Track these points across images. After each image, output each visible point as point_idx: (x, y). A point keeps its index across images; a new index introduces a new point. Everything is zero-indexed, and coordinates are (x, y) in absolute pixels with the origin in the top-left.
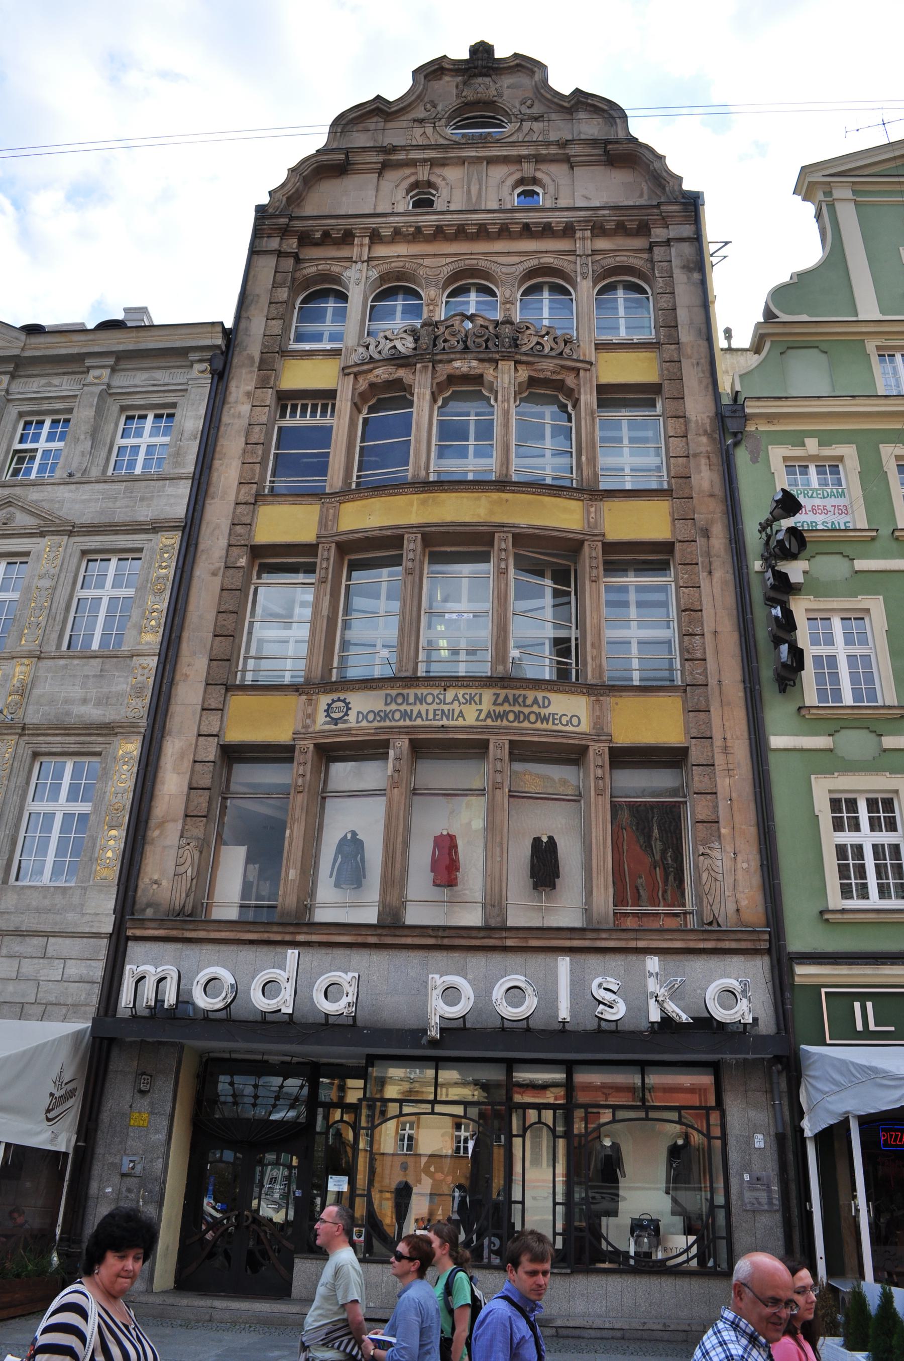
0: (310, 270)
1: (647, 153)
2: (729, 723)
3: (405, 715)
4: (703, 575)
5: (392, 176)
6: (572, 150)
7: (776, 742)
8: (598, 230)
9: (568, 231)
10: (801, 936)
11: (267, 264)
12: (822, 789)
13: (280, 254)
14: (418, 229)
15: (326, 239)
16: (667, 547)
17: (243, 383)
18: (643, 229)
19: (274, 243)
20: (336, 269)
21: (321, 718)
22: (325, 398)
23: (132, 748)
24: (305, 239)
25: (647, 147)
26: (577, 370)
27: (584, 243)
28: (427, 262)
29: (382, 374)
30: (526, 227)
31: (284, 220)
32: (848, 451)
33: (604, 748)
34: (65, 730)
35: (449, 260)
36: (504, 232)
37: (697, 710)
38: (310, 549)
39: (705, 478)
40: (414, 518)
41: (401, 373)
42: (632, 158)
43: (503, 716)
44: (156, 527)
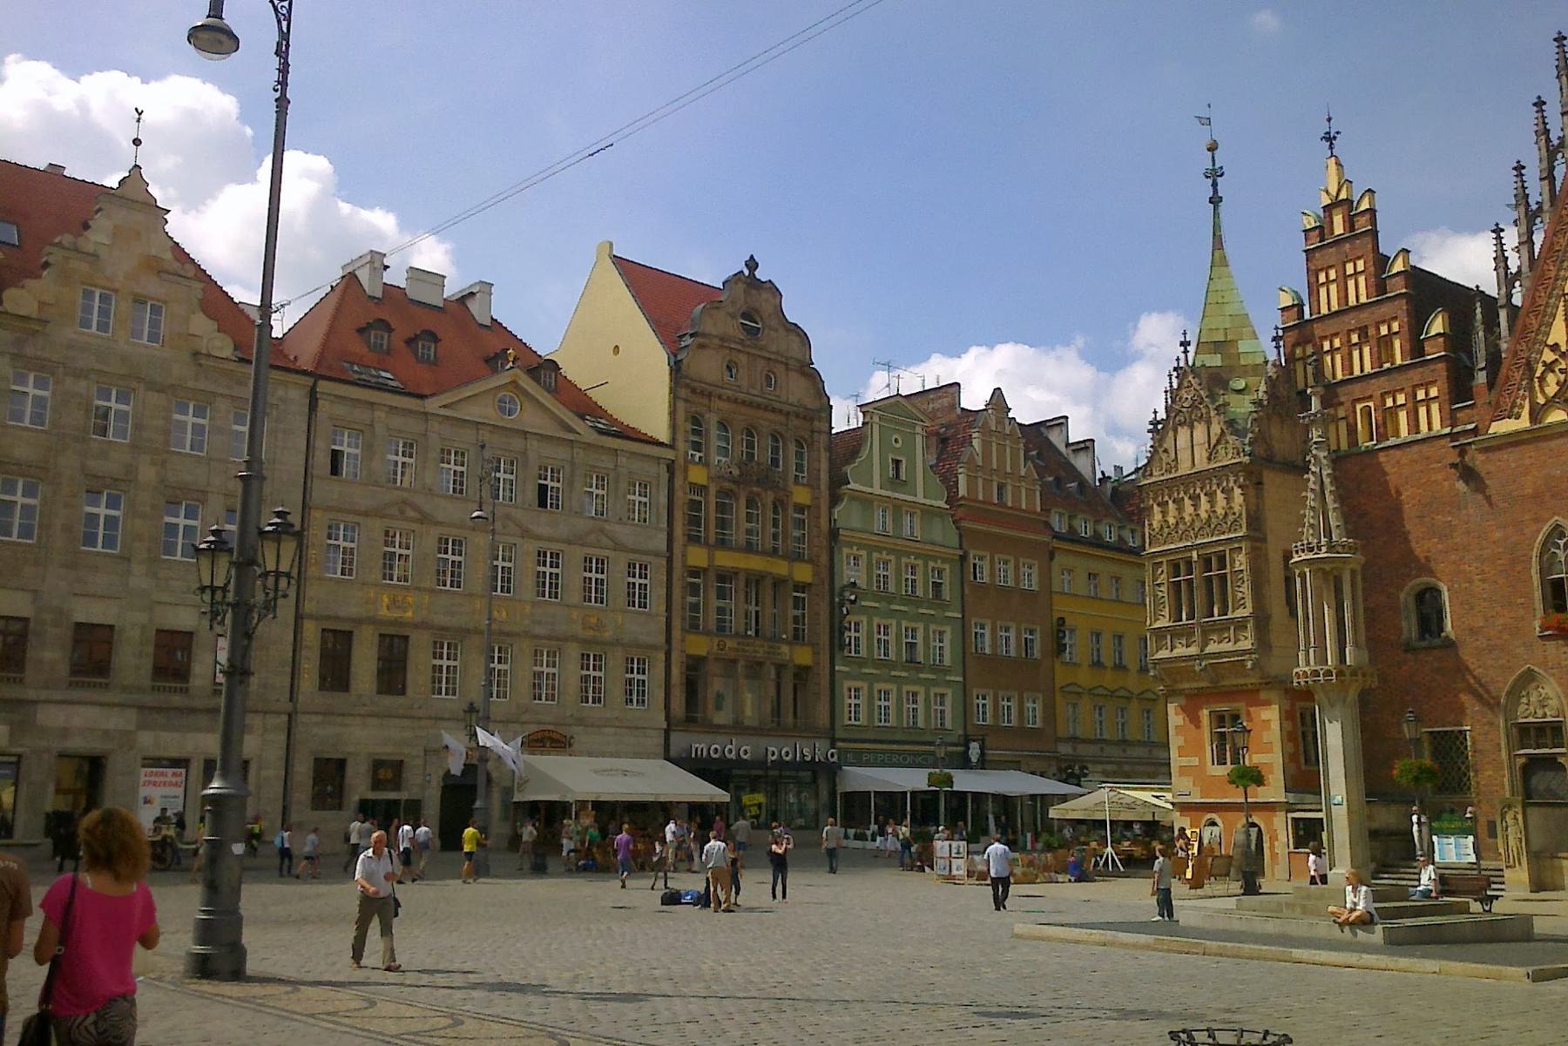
6: (791, 362)
9: (788, 414)
10: (839, 734)
11: (681, 405)
12: (847, 684)
13: (686, 401)
17: (678, 482)
19: (683, 393)
22: (702, 489)
23: (662, 656)
24: (694, 391)
29: (727, 485)
34: (639, 646)
37: (816, 654)
38: (705, 570)
39: (824, 559)
40: (742, 565)
44: (657, 554)
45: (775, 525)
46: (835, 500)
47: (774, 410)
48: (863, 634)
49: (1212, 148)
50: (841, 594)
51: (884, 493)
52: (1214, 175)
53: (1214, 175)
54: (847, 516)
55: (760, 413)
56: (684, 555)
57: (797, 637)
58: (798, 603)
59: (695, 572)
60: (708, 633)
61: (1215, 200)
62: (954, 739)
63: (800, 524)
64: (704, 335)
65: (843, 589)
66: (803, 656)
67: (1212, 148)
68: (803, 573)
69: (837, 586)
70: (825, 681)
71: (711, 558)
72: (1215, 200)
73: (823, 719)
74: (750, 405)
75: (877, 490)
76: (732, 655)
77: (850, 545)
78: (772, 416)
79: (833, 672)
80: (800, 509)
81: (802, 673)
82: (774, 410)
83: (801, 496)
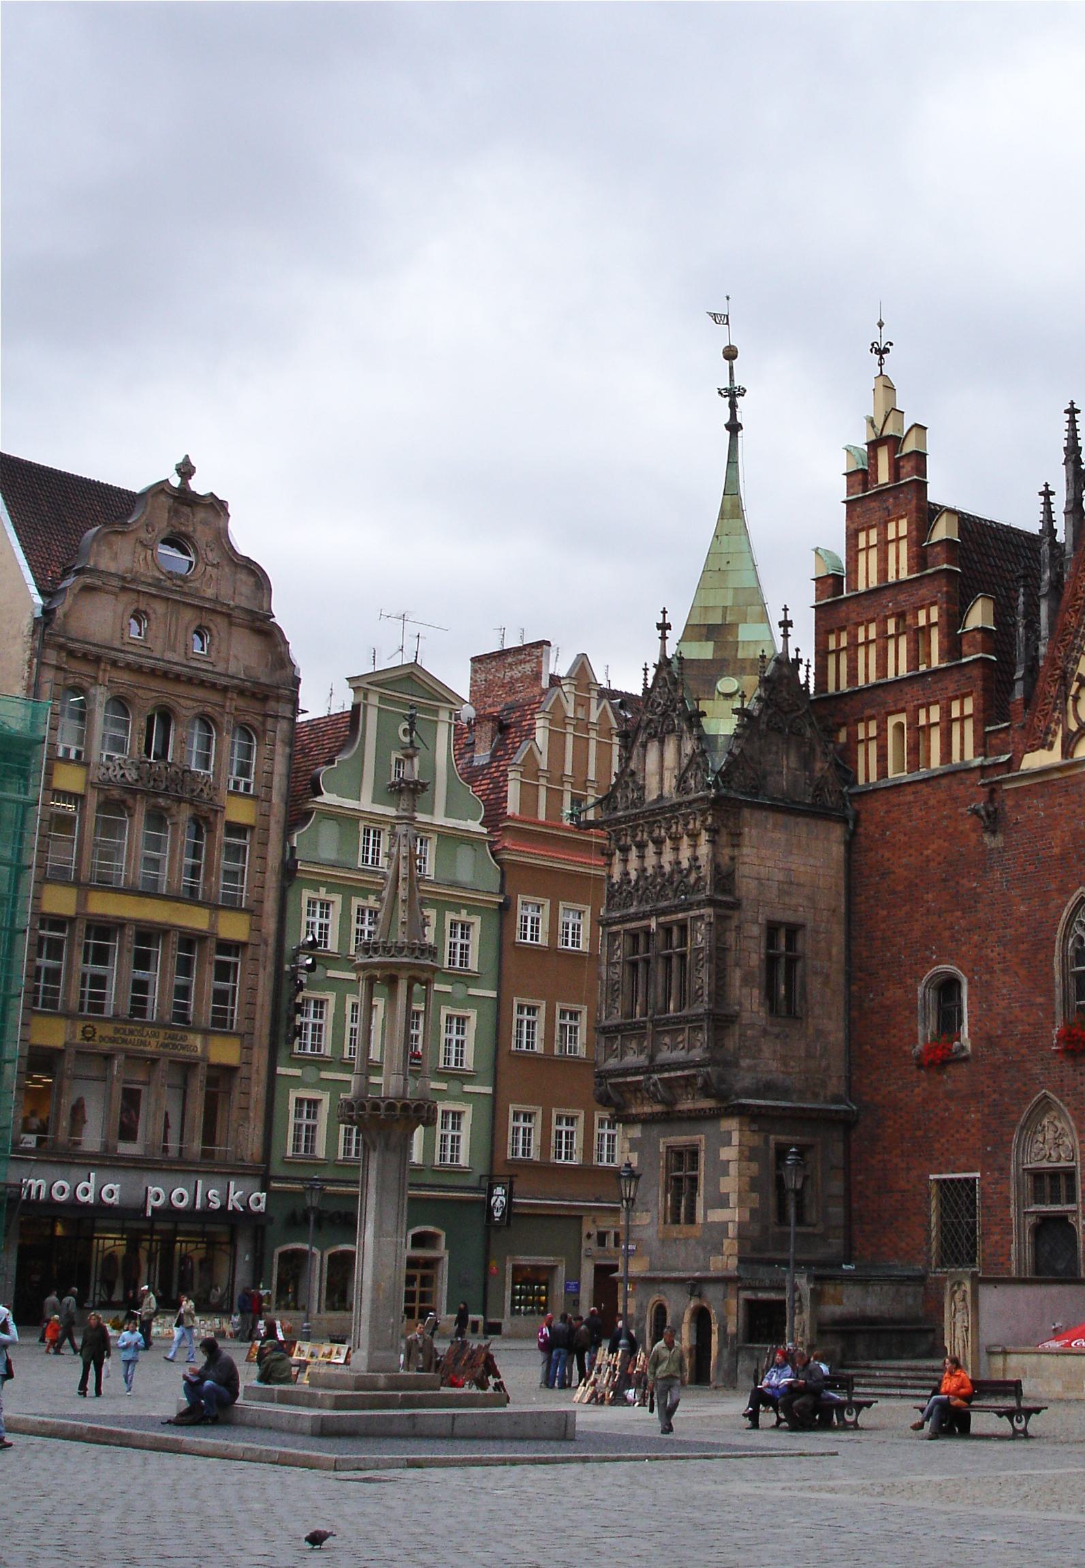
0: (71, 681)
1: (276, 632)
2: (260, 1057)
3: (124, 1041)
4: (261, 969)
5: (125, 598)
6: (236, 613)
7: (281, 1070)
8: (242, 692)
9: (225, 689)
10: (277, 1169)
11: (49, 675)
13: (58, 668)
14: (141, 667)
15: (85, 657)
16: (244, 945)
18: (266, 699)
19: (52, 657)
20: (86, 685)
21: (79, 1035)
24: (71, 654)
25: (279, 629)
26: (217, 811)
27: (233, 702)
28: (140, 692)
29: (116, 794)
30: (203, 681)
31: (62, 640)
32: (337, 898)
33: (205, 1064)
35: (154, 694)
36: (190, 681)
38: (73, 920)
39: (270, 906)
41: (127, 797)
42: (267, 632)
43: (166, 1046)
45: (196, 852)
46: (297, 817)
47: (202, 684)
48: (328, 1021)
49: (730, 354)
50: (294, 959)
51: (379, 809)
52: (733, 394)
53: (733, 394)
54: (320, 844)
55: (181, 689)
56: (37, 898)
57: (220, 1021)
58: (224, 972)
59: (57, 922)
60: (67, 1015)
61: (734, 427)
62: (472, 1181)
63: (236, 853)
64: (94, 571)
65: (298, 952)
66: (225, 1052)
67: (730, 354)
68: (234, 927)
69: (290, 945)
70: (258, 1091)
71: (82, 901)
72: (734, 427)
73: (251, 1142)
74: (165, 675)
75: (366, 803)
76: (106, 1046)
77: (315, 885)
78: (199, 693)
79: (272, 1075)
80: (235, 829)
81: (222, 1076)
82: (202, 684)
83: (240, 811)
